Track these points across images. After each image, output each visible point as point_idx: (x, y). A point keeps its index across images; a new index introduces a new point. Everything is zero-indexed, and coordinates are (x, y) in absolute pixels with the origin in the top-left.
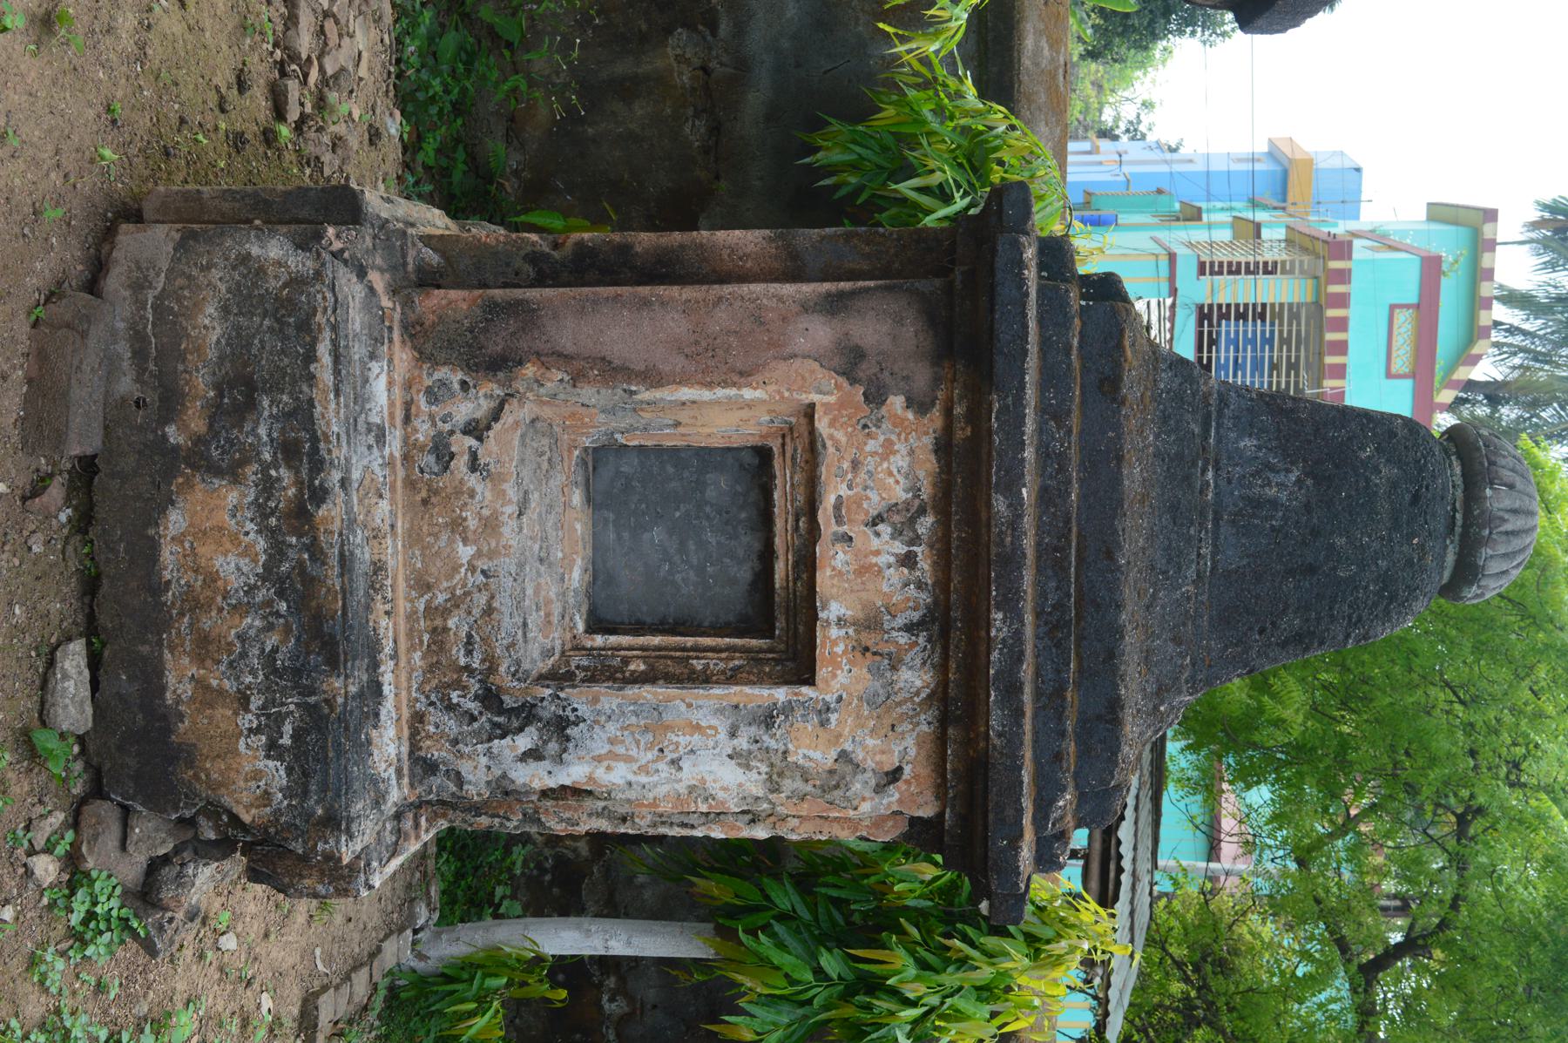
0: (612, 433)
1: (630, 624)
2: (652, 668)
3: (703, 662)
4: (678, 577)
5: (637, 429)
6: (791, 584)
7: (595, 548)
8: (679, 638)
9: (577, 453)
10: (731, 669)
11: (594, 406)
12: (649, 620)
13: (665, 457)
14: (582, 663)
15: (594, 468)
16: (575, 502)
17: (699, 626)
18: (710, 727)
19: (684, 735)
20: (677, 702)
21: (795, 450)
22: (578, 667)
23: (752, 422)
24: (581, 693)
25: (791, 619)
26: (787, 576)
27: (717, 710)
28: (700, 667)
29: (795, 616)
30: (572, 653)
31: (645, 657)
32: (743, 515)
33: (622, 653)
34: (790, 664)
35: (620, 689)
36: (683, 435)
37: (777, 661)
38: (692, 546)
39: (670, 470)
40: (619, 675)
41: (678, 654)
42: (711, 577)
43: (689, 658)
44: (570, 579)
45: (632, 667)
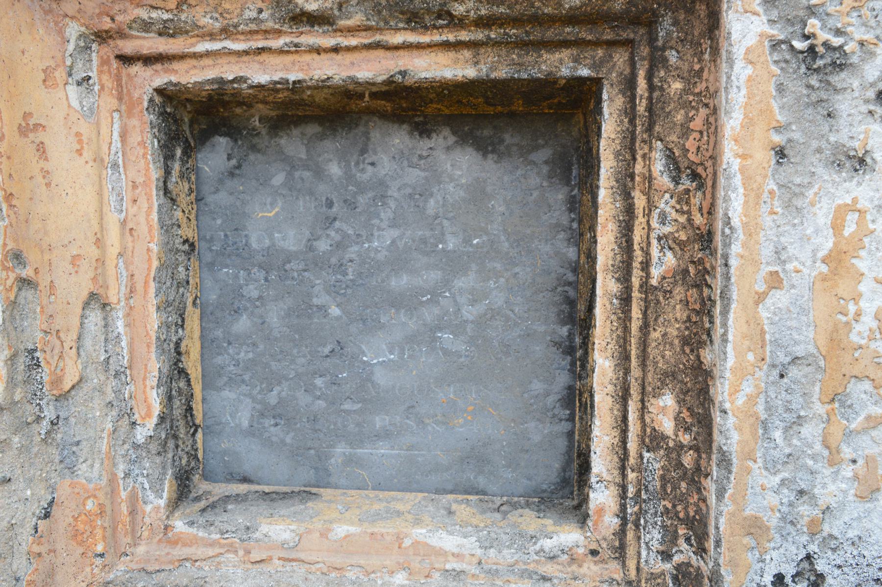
0: (136, 446)
1: (571, 418)
2: (669, 376)
3: (655, 252)
4: (469, 312)
5: (117, 392)
6: (464, 36)
7: (406, 488)
8: (598, 311)
9: (179, 525)
10: (676, 180)
11: (53, 489)
12: (563, 379)
13: (219, 333)
14: (656, 545)
15: (245, 480)
16: (287, 536)
17: (575, 269)
18: (837, 226)
19: (856, 298)
20: (764, 313)
21: (146, 26)
22: (666, 556)
23: (84, 128)
24: (733, 564)
25: (550, 34)
26: (446, 45)
27: (788, 205)
28: (670, 259)
29: (537, 20)
30: (632, 564)
31: (643, 392)
32: (335, 169)
33: (632, 445)
34: (665, 28)
35: (725, 461)
36: (132, 291)
37: (657, 61)
38: (401, 282)
39: (243, 324)
40: (688, 459)
41: (636, 313)
42: (467, 241)
43: (645, 287)
44: (458, 556)
45: (667, 426)
